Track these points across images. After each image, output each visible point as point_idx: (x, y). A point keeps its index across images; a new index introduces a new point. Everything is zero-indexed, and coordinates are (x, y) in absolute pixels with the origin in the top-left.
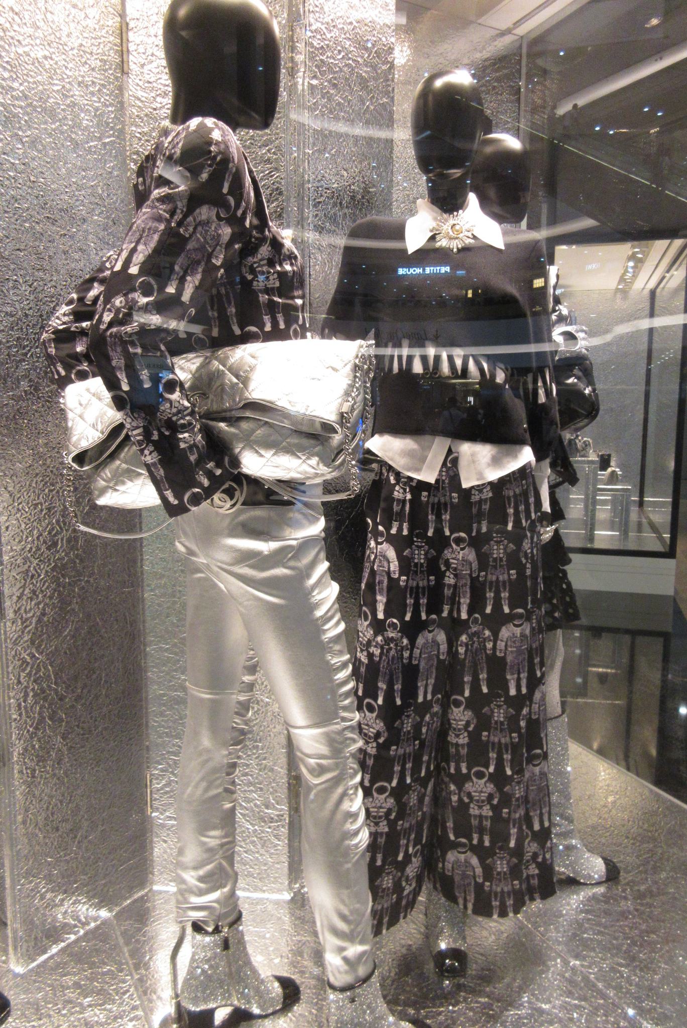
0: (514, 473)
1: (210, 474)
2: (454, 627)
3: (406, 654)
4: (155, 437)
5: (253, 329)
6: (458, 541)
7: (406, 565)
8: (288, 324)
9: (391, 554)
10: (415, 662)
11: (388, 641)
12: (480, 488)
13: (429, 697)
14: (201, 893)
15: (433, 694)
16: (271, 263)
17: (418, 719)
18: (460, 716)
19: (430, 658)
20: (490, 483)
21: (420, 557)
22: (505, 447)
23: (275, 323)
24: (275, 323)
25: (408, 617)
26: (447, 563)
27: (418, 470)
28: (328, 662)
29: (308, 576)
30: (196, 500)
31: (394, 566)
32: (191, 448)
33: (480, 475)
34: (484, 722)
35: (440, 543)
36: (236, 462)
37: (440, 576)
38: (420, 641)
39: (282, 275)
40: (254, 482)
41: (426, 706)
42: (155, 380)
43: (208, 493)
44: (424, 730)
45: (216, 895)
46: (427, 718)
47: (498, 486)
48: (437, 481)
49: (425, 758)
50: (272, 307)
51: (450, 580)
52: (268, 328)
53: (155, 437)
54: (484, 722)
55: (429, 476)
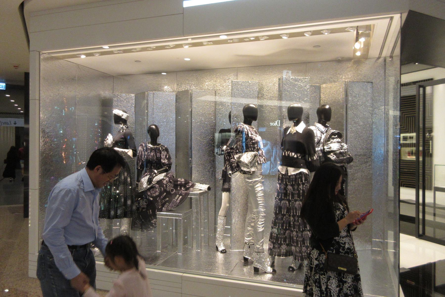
0: (298, 173)
1: (236, 169)
2: (289, 201)
3: (279, 204)
4: (230, 164)
5: (248, 150)
6: (289, 185)
7: (280, 187)
8: (254, 149)
9: (278, 186)
10: (281, 206)
11: (276, 201)
12: (292, 175)
13: (285, 213)
14: (247, 238)
15: (286, 213)
16: (251, 141)
17: (282, 216)
18: (292, 218)
19: (285, 206)
20: (294, 175)
21: (283, 187)
22: (296, 169)
23: (251, 149)
24: (251, 149)
25: (280, 197)
26: (288, 189)
27: (282, 172)
28: (257, 200)
29: (255, 186)
30: (234, 172)
31: (279, 188)
32: (234, 166)
33: (291, 173)
34: (295, 220)
35: (286, 185)
36: (240, 168)
37: (287, 191)
38: (282, 202)
39: (253, 143)
40: (242, 170)
41: (284, 215)
42: (229, 158)
43: (236, 172)
44: (284, 219)
45: (249, 239)
46: (285, 217)
47: (296, 175)
48: (285, 174)
49: (285, 225)
50: (251, 147)
51: (288, 192)
52: (250, 150)
53: (230, 164)
54: (295, 220)
55: (283, 173)
